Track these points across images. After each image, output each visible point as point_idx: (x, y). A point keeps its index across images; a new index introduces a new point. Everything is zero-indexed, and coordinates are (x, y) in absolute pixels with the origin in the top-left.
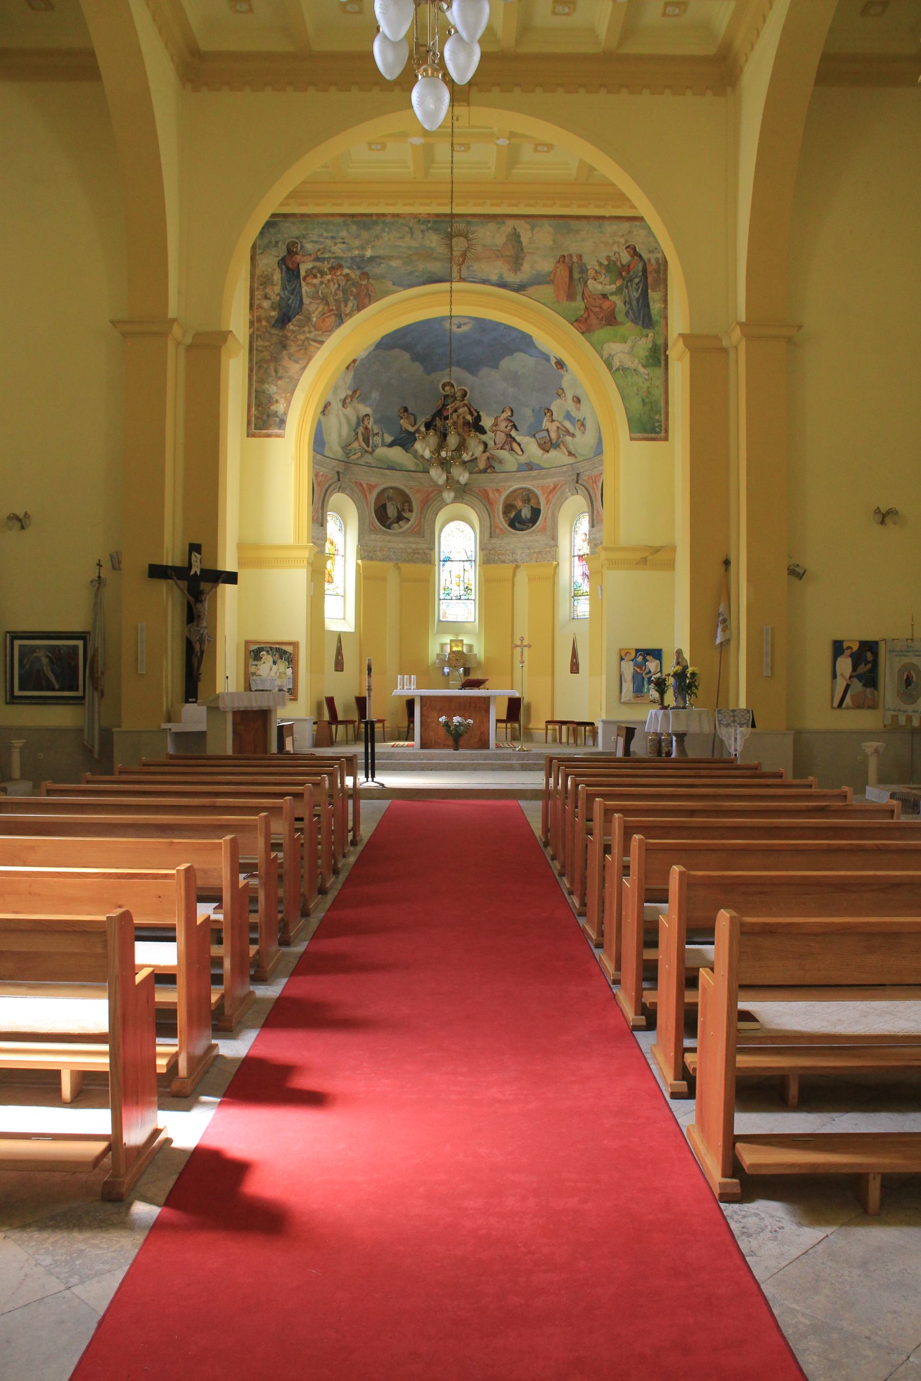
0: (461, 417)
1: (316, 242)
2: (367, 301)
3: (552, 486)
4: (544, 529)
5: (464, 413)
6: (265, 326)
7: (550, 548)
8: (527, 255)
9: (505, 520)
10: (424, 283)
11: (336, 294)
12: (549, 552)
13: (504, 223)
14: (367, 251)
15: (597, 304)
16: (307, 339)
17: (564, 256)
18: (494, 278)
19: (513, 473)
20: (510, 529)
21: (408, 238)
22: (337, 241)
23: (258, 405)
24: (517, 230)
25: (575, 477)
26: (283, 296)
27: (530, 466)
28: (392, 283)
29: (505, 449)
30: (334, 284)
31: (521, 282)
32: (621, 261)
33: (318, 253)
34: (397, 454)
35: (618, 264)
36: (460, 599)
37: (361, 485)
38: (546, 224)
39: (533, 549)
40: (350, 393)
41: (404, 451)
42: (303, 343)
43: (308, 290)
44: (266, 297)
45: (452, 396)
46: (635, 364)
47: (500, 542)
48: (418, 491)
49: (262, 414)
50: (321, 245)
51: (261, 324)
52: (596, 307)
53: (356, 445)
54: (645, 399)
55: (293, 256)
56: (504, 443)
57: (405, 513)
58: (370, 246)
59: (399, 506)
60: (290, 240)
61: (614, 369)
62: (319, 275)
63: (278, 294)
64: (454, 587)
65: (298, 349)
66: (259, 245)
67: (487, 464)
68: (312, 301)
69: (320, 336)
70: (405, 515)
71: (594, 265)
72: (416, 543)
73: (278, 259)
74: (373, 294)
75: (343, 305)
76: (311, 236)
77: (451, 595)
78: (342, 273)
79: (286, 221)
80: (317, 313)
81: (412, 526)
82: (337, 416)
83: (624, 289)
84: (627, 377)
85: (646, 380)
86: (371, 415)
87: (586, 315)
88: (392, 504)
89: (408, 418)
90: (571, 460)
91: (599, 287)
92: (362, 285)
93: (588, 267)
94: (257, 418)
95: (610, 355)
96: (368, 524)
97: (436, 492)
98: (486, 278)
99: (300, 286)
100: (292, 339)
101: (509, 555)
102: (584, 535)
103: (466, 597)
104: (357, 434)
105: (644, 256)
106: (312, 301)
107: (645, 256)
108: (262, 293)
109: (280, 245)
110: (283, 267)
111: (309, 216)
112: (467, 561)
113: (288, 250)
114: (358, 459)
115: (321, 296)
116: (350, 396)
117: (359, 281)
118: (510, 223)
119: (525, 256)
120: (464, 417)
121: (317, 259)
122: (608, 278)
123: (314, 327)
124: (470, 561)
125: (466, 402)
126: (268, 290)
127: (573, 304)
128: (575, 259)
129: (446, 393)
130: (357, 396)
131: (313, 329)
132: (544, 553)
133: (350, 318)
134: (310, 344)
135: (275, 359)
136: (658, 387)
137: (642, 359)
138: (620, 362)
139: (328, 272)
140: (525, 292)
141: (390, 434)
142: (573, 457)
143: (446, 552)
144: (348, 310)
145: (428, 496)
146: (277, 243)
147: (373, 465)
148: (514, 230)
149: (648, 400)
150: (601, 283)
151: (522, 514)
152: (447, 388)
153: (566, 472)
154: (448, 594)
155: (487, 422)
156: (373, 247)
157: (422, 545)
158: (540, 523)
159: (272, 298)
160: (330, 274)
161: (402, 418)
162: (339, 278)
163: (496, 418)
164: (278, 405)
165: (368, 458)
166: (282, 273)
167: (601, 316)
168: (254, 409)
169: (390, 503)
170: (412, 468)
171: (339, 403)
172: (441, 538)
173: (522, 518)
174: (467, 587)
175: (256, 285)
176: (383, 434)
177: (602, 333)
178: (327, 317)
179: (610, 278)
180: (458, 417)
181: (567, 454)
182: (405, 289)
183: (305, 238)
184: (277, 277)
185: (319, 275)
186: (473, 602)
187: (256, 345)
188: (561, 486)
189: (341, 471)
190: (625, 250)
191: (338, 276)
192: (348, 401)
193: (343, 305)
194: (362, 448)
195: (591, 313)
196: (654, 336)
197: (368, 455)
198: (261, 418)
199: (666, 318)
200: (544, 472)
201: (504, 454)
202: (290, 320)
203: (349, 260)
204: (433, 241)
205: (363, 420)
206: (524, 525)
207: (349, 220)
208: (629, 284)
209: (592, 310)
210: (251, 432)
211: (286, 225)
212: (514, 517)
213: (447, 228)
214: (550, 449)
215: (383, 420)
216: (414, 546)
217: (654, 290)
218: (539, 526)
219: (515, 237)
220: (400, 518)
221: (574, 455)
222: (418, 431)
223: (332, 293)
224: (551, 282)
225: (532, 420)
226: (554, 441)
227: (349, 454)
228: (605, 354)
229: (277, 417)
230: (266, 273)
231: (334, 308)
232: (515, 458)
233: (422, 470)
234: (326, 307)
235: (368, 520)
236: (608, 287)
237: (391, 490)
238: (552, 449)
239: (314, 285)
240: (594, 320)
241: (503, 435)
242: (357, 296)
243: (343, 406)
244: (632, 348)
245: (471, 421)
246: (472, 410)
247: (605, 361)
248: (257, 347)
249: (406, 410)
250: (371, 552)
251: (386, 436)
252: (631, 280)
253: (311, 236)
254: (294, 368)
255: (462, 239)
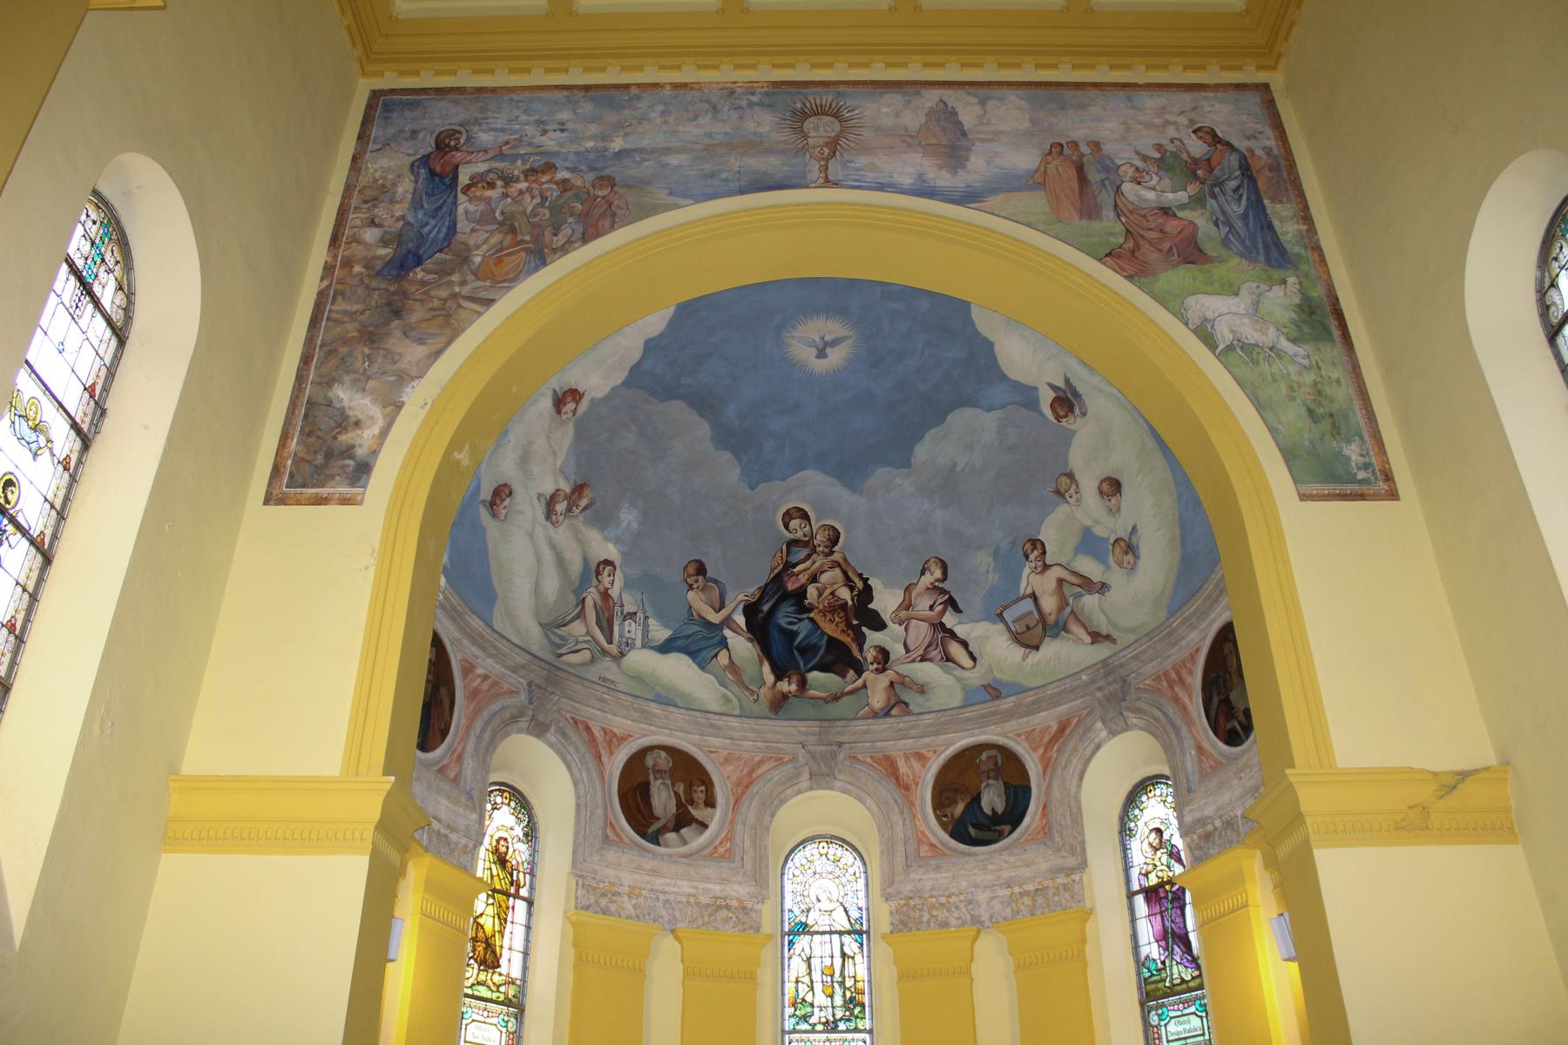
0: (827, 592)
1: (502, 130)
2: (607, 224)
3: (1054, 726)
4: (1046, 832)
5: (833, 584)
6: (362, 273)
7: (1068, 876)
8: (978, 144)
9: (944, 826)
10: (742, 192)
11: (534, 213)
12: (1064, 885)
13: (919, 93)
14: (614, 141)
15: (1153, 225)
16: (455, 296)
17: (1062, 146)
18: (907, 181)
19: (954, 712)
20: (953, 843)
21: (706, 120)
22: (547, 128)
23: (308, 432)
24: (950, 105)
25: (1117, 686)
26: (411, 220)
27: (994, 691)
28: (667, 191)
29: (930, 660)
30: (533, 198)
31: (967, 187)
32: (1188, 153)
33: (504, 148)
34: (678, 670)
35: (1184, 156)
36: (835, 1030)
37: (588, 729)
38: (1012, 96)
39: (1020, 886)
40: (566, 488)
41: (696, 667)
42: (444, 304)
43: (472, 208)
44: (372, 223)
45: (806, 544)
46: (1270, 336)
47: (932, 875)
48: (727, 760)
49: (316, 452)
50: (511, 134)
51: (351, 271)
52: (1149, 230)
53: (578, 628)
54: (1313, 406)
55: (446, 153)
56: (929, 645)
57: (696, 808)
58: (621, 134)
59: (681, 789)
60: (442, 129)
61: (1221, 347)
62: (499, 183)
63: (403, 218)
64: (820, 999)
65: (429, 316)
66: (375, 138)
67: (889, 699)
68: (478, 227)
69: (484, 291)
70: (694, 812)
71: (1130, 159)
72: (723, 881)
73: (414, 158)
74: (620, 212)
75: (548, 233)
76: (491, 120)
77: (812, 1020)
78: (553, 178)
79: (440, 100)
80: (485, 247)
81: (714, 839)
82: (531, 536)
83: (1208, 197)
84: (1258, 363)
85: (1306, 367)
86: (617, 564)
87: (1130, 245)
88: (664, 783)
89: (703, 589)
90: (1103, 651)
91: (1151, 195)
92: (598, 197)
93: (1119, 162)
94: (298, 461)
95: (1206, 319)
96: (600, 823)
97: (772, 764)
98: (886, 180)
99: (455, 203)
100: (418, 297)
101: (957, 908)
102: (1153, 835)
103: (852, 1025)
104: (584, 599)
105: (1235, 143)
106: (478, 227)
107: (1241, 144)
108: (367, 215)
109: (421, 136)
110: (422, 171)
111: (493, 90)
112: (849, 933)
113: (437, 144)
114: (583, 664)
115: (500, 218)
116: (568, 497)
117: (591, 189)
118: (931, 97)
119: (973, 145)
120: (833, 593)
121: (500, 156)
122: (1166, 182)
123: (475, 274)
124: (860, 933)
125: (836, 557)
126: (381, 212)
127: (1095, 225)
128: (1085, 149)
129: (791, 536)
130: (584, 502)
131: (471, 277)
132: (1051, 892)
133: (559, 258)
134: (459, 306)
135: (371, 337)
136: (1338, 381)
137: (1285, 327)
138: (1232, 331)
139: (522, 177)
140: (982, 204)
141: (664, 620)
142: (1107, 643)
143: (797, 912)
144: (561, 239)
145: (753, 771)
146: (414, 133)
147: (620, 687)
148: (941, 106)
149: (1322, 410)
150: (1154, 189)
151: (983, 804)
152: (794, 523)
153: (1087, 684)
154: (805, 1018)
155: (886, 601)
156: (626, 134)
157: (737, 887)
158: (1031, 822)
159: (385, 223)
160: (526, 180)
161: (691, 587)
162: (546, 186)
163: (908, 590)
164: (359, 432)
165: (607, 667)
166: (416, 182)
167: (1166, 246)
168: (295, 440)
169: (660, 781)
170: (714, 705)
171: (536, 501)
172: (786, 877)
173: (985, 814)
174: (852, 999)
175: (354, 202)
176: (646, 618)
177: (1175, 278)
178: (505, 255)
179: (1170, 179)
180: (820, 595)
181: (1088, 639)
182: (696, 203)
183: (480, 125)
184: (405, 188)
185: (499, 183)
186: (867, 1037)
187: (330, 311)
188: (1079, 720)
189: (537, 681)
190: (1193, 136)
191: (543, 183)
192: (561, 507)
193: (548, 233)
194: (597, 643)
195: (1142, 242)
196: (1300, 283)
197: (607, 663)
198: (308, 462)
199: (1317, 248)
200: (1030, 698)
201: (929, 672)
202: (419, 261)
203: (571, 157)
204: (764, 123)
205: (598, 573)
206: (991, 830)
207: (579, 95)
208: (1217, 190)
209: (1142, 237)
210: (276, 492)
211: (442, 104)
212: (964, 811)
213: (795, 103)
214: (1041, 642)
215: (644, 583)
216: (716, 888)
217: (1273, 200)
218: (1027, 829)
219: (947, 115)
220: (683, 820)
221: (1108, 637)
222: (728, 622)
223: (525, 213)
224: (1042, 185)
225: (993, 578)
226: (1051, 619)
227: (560, 646)
228: (1194, 317)
229: (352, 457)
230: (381, 181)
231: (527, 238)
232: (952, 674)
233: (737, 712)
234: (509, 238)
235: (600, 812)
236: (1171, 196)
237: (663, 754)
238: (1047, 639)
239: (488, 201)
240: (1154, 257)
241: (924, 625)
242: (584, 217)
243: (548, 517)
244: (1256, 304)
245: (850, 603)
246: (850, 574)
247: (1195, 331)
248: (334, 316)
249: (701, 569)
250: (603, 895)
251: (651, 621)
252: (1220, 184)
253: (491, 120)
254: (414, 353)
255: (827, 119)
